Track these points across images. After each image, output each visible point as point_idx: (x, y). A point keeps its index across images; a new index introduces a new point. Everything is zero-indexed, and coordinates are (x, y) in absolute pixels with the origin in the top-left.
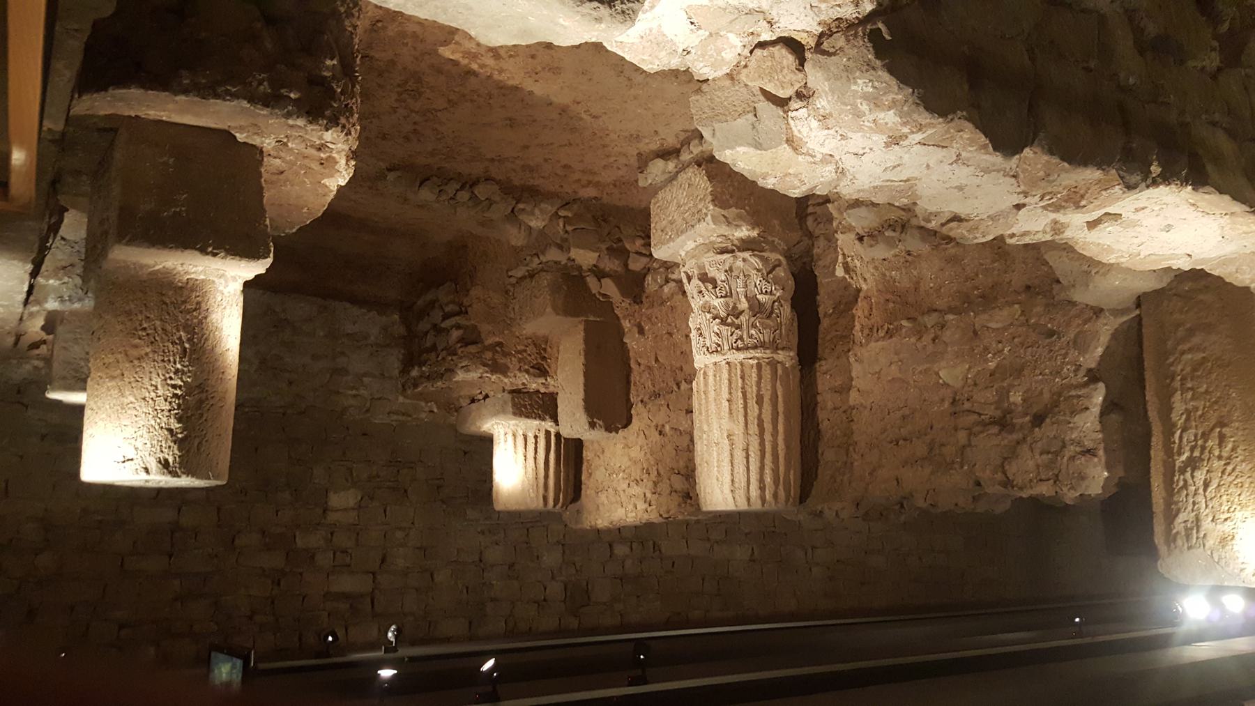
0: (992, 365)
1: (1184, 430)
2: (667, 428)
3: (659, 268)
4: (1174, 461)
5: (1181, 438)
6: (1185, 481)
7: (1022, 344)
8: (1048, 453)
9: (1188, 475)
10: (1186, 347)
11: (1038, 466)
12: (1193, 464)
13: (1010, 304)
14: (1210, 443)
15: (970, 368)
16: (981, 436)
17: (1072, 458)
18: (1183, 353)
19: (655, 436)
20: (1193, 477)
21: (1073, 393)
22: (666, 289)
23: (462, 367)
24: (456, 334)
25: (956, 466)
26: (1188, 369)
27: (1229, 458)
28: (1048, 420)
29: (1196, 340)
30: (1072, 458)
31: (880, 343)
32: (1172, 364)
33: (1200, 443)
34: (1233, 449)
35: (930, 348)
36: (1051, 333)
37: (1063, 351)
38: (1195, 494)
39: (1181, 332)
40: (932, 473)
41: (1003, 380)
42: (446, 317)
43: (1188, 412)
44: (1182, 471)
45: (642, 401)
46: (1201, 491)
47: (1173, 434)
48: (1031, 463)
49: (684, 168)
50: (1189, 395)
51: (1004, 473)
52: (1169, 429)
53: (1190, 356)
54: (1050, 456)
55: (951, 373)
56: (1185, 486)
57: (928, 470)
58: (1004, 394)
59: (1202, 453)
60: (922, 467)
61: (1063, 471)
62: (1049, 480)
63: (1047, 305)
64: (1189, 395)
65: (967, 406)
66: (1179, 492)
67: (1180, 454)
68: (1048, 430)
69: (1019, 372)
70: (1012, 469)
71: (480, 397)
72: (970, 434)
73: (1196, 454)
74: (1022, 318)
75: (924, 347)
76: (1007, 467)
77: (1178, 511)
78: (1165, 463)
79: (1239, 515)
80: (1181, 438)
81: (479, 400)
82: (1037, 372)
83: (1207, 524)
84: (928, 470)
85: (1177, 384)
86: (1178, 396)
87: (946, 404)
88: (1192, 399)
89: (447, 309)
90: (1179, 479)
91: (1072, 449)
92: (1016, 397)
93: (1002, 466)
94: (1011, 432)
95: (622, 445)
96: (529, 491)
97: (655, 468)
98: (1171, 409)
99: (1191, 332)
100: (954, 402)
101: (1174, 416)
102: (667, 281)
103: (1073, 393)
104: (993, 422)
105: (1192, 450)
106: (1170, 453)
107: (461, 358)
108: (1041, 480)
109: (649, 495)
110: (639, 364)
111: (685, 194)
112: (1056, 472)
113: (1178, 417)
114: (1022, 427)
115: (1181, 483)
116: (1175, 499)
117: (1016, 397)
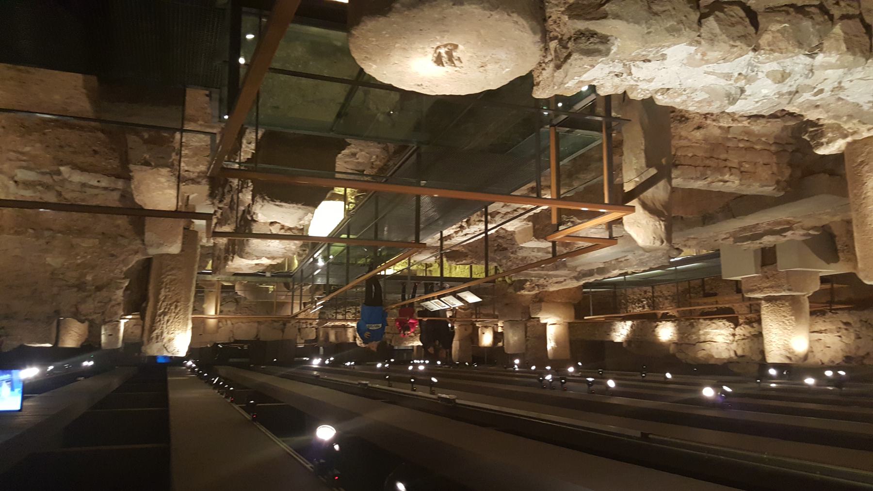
0: (79, 261)
1: (163, 301)
5: (161, 304)
6: (160, 319)
9: (162, 317)
12: (164, 314)
14: (172, 308)
17: (113, 306)
18: (168, 275)
20: (163, 318)
21: (118, 281)
26: (168, 282)
27: (177, 313)
28: (104, 290)
29: (174, 272)
30: (113, 306)
31: (9, 236)
34: (180, 310)
36: (112, 255)
38: (163, 324)
39: (169, 268)
43: (166, 296)
44: (160, 316)
46: (165, 323)
47: (159, 302)
48: (92, 306)
50: (167, 290)
51: (77, 309)
52: (157, 301)
53: (170, 277)
54: (103, 304)
55: (54, 260)
59: (169, 310)
64: (167, 290)
65: (61, 276)
66: (157, 322)
67: (160, 310)
68: (104, 293)
69: (93, 267)
73: (166, 310)
77: (155, 330)
78: (153, 312)
79: (177, 332)
80: (161, 304)
83: (165, 335)
86: (163, 290)
88: (169, 291)
90: (158, 319)
91: (113, 303)
92: (89, 278)
94: (84, 292)
98: (160, 294)
99: (172, 269)
100: (52, 273)
101: (160, 296)
103: (118, 281)
104: (73, 286)
105: (165, 309)
106: (155, 308)
108: (96, 313)
113: (161, 297)
115: (158, 320)
116: (155, 325)
117: (89, 278)
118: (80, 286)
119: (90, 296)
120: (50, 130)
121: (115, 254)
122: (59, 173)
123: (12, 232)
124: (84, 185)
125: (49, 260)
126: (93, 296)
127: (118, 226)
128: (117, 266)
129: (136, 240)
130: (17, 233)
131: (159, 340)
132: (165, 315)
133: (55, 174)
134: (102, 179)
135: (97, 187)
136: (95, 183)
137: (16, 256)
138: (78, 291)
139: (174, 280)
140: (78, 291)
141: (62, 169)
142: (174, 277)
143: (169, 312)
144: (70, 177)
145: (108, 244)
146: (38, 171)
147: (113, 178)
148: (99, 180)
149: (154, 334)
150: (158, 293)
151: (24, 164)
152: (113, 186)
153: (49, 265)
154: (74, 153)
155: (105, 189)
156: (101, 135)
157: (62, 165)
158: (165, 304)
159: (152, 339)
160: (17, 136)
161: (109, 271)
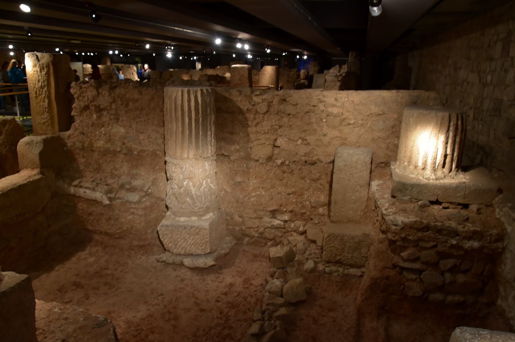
0: (103, 129)
1: (45, 97)
2: (299, 142)
3: (291, 231)
4: (47, 88)
5: (45, 95)
7: (92, 133)
8: (83, 96)
9: (43, 84)
10: (45, 120)
11: (87, 92)
12: (42, 87)
13: (97, 147)
15: (111, 130)
16: (105, 105)
19: (311, 139)
20: (42, 83)
22: (286, 217)
23: (396, 225)
24: (404, 254)
25: (116, 96)
29: (43, 121)
31: (147, 149)
32: (49, 116)
33: (41, 93)
35: (126, 141)
36: (83, 134)
37: (79, 127)
38: (41, 79)
39: (47, 124)
40: (125, 95)
41: (98, 123)
42: (420, 272)
43: (44, 101)
44: (45, 86)
45: (322, 162)
46: (40, 79)
47: (47, 96)
48: (89, 93)
49: (179, 254)
50: (44, 106)
52: (49, 97)
55: (119, 130)
56: (44, 82)
57: (127, 96)
58: (99, 118)
60: (129, 98)
61: (78, 90)
62: (84, 87)
63: (85, 143)
64: (44, 106)
65: (112, 117)
66: (45, 80)
67: (46, 90)
68: (83, 104)
70: (95, 92)
71: (444, 205)
72: (111, 106)
73: (41, 90)
74: (93, 142)
75: (128, 142)
76: (96, 93)
77: (46, 74)
79: (32, 72)
81: (448, 203)
82: (87, 123)
83: (39, 70)
84: (127, 96)
85: (47, 110)
86: (47, 106)
87: (120, 120)
88: (43, 105)
89: (414, 277)
93: (99, 94)
95: (348, 140)
96: (413, 123)
97: (314, 120)
99: (44, 123)
100: (118, 119)
102: (285, 221)
105: (42, 91)
106: (49, 90)
107: (396, 233)
109: (321, 107)
110: (321, 184)
111: (180, 243)
112: (81, 90)
113: (47, 101)
114: (92, 106)
115: (45, 82)
116: (47, 78)
117: (95, 116)
118: (99, 110)
119: (91, 102)
120: (117, 231)
121: (82, 135)
122: (110, 199)
123: (147, 152)
124: (94, 190)
125: (122, 130)
126: (89, 101)
127: (84, 157)
128: (79, 126)
129: (70, 146)
130: (144, 151)
131: (42, 66)
132: (41, 86)
133: (113, 198)
134: (84, 194)
135: (86, 188)
136: (88, 191)
137: (142, 133)
138: (99, 106)
139: (41, 115)
140: (99, 106)
141: (108, 202)
142: (42, 117)
143: (39, 89)
144: (102, 196)
145: (87, 143)
146: (123, 200)
147: (77, 195)
148: (85, 194)
149: (46, 70)
150: (50, 103)
151: (133, 206)
152: (76, 189)
153: (121, 126)
154: (103, 215)
155: (81, 187)
156: (90, 228)
157: (108, 205)
158: (44, 95)
159: (46, 67)
160: (136, 227)
161: (83, 122)
